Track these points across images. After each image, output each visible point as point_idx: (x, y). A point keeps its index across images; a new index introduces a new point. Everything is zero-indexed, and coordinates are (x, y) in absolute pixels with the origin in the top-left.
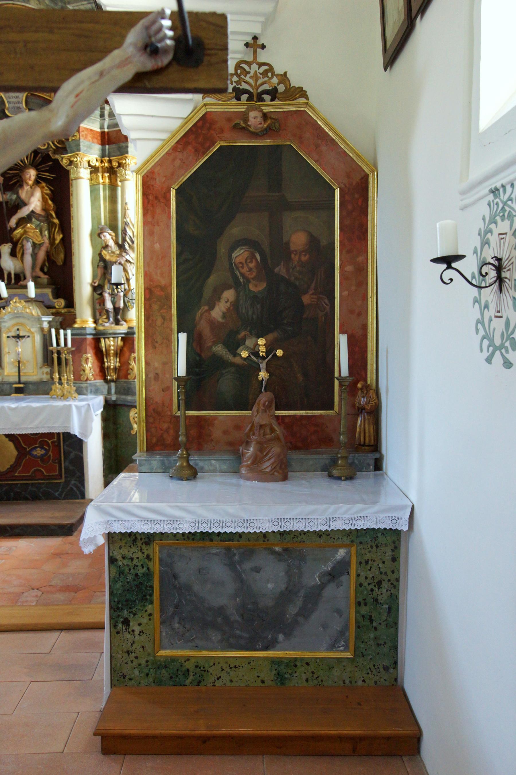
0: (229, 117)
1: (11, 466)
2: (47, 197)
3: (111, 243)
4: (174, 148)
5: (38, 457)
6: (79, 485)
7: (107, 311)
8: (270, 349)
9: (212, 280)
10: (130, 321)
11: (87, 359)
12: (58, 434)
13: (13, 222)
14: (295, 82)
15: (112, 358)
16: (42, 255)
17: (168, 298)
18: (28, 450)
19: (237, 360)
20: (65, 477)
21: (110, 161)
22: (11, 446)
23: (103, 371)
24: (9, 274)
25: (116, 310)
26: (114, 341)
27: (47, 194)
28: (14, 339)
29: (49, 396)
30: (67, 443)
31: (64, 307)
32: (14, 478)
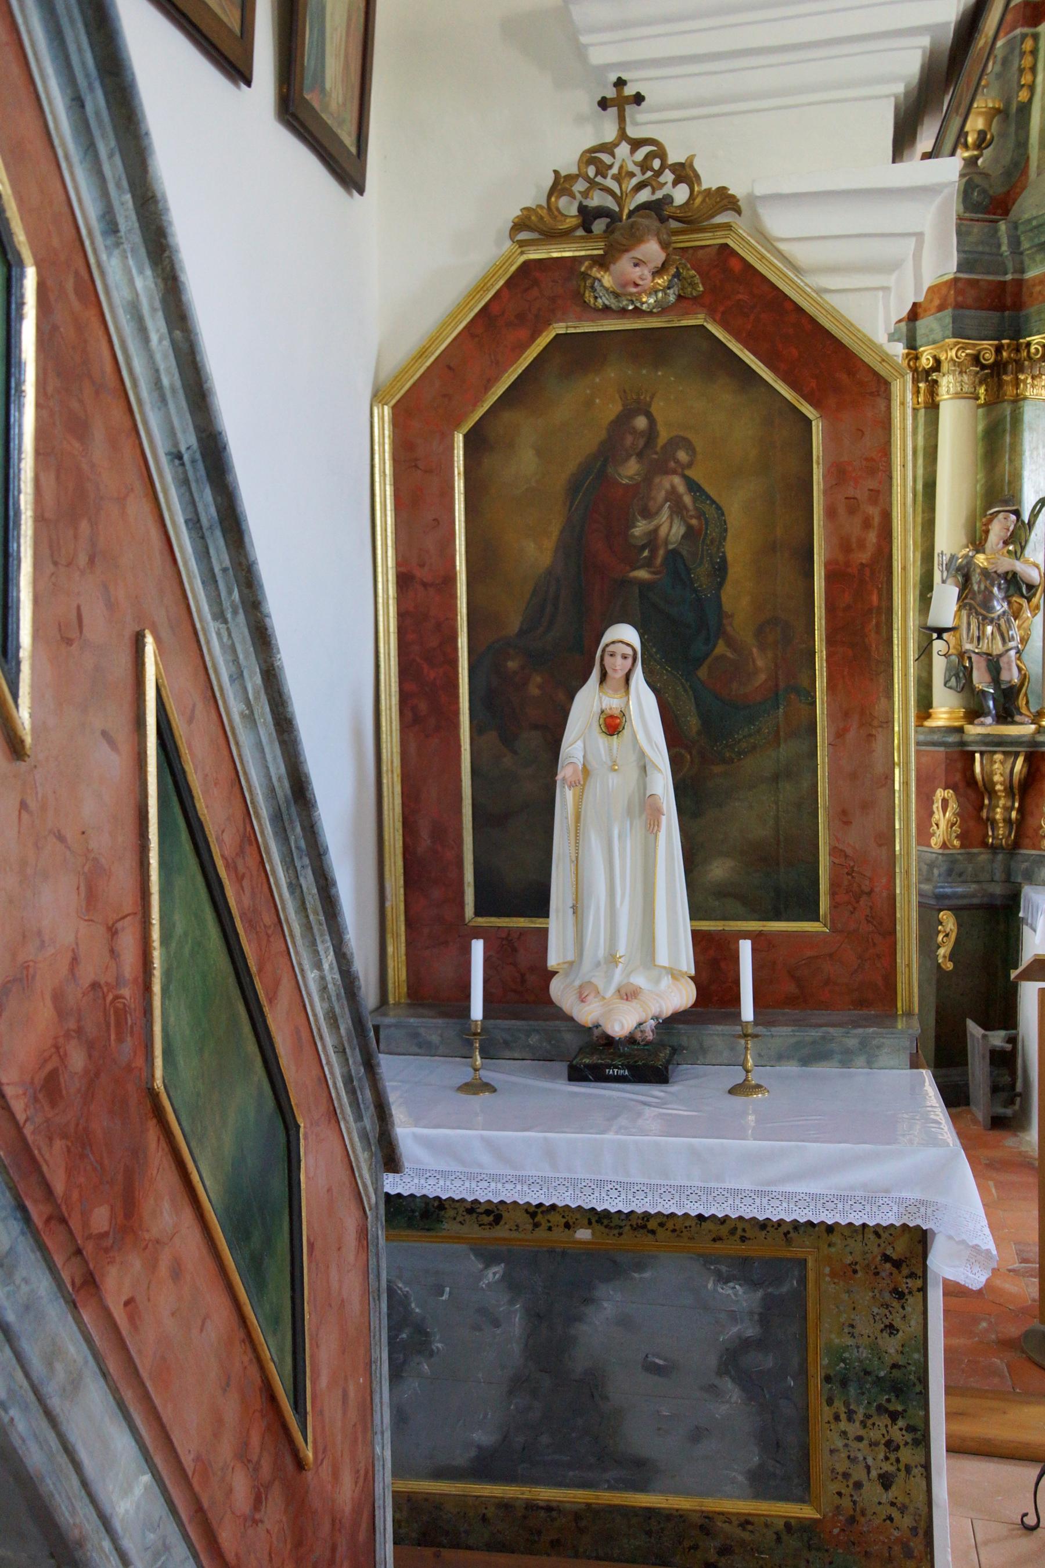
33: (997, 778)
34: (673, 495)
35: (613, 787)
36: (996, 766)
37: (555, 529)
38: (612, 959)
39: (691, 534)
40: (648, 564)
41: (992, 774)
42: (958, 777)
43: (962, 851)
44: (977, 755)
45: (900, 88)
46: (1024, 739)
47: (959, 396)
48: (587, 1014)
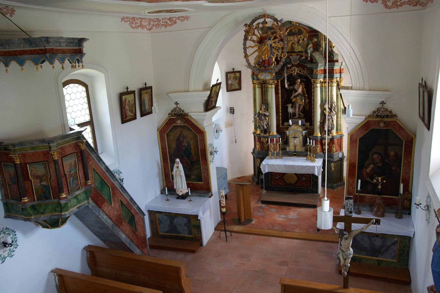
0: (375, 122)
4: (359, 129)
8: (382, 180)
9: (367, 162)
11: (318, 147)
13: (292, 97)
14: (394, 113)
16: (302, 107)
17: (356, 166)
19: (373, 182)
22: (295, 176)
24: (291, 113)
29: (305, 158)
48: (178, 193)
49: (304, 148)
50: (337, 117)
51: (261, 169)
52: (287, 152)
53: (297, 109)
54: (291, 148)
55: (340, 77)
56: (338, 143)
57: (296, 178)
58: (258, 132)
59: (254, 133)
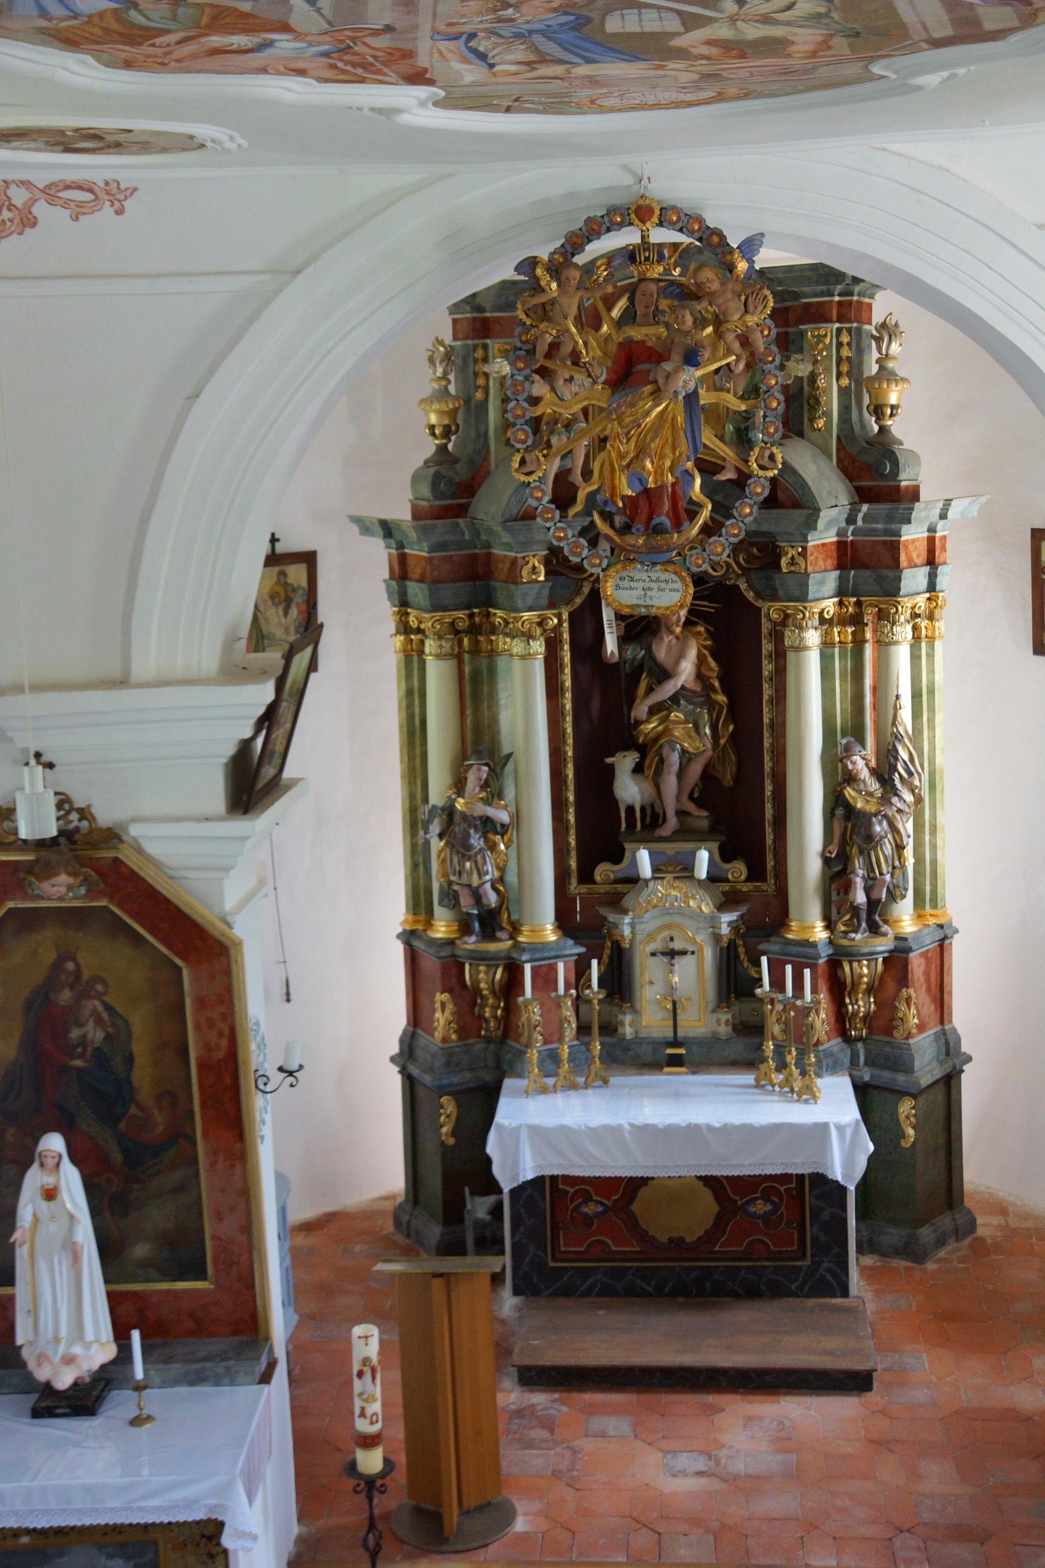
1: (706, 1232)
2: (706, 652)
3: (865, 774)
5: (759, 1217)
6: (838, 1271)
7: (855, 910)
10: (896, 921)
12: (801, 1177)
13: (640, 710)
15: (860, 995)
16: (696, 770)
18: (739, 1203)
20: (812, 1255)
21: (859, 604)
22: (707, 1194)
23: (841, 1021)
25: (873, 904)
26: (868, 966)
27: (705, 647)
28: (665, 960)
30: (815, 1192)
31: (747, 880)
32: (712, 1256)
33: (483, 985)
34: (95, 1013)
35: (52, 1230)
36: (481, 976)
37: (18, 1034)
38: (57, 1340)
39: (108, 1037)
40: (81, 1056)
41: (478, 982)
42: (454, 981)
43: (460, 1043)
44: (467, 967)
45: (225, 760)
46: (502, 955)
47: (439, 656)
48: (42, 1374)
49: (725, 1016)
50: (918, 826)
51: (488, 1161)
52: (625, 1045)
53: (670, 784)
54: (647, 1018)
55: (932, 587)
56: (927, 974)
57: (708, 1205)
58: (442, 928)
59: (408, 937)
